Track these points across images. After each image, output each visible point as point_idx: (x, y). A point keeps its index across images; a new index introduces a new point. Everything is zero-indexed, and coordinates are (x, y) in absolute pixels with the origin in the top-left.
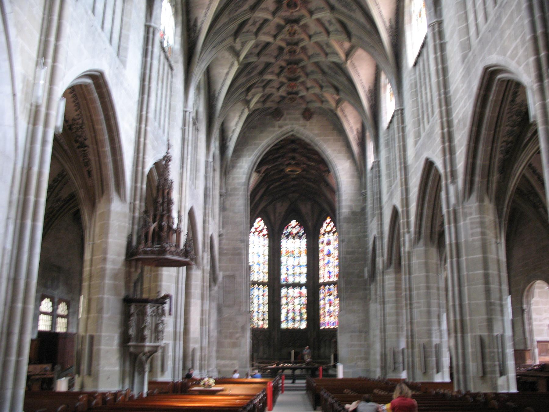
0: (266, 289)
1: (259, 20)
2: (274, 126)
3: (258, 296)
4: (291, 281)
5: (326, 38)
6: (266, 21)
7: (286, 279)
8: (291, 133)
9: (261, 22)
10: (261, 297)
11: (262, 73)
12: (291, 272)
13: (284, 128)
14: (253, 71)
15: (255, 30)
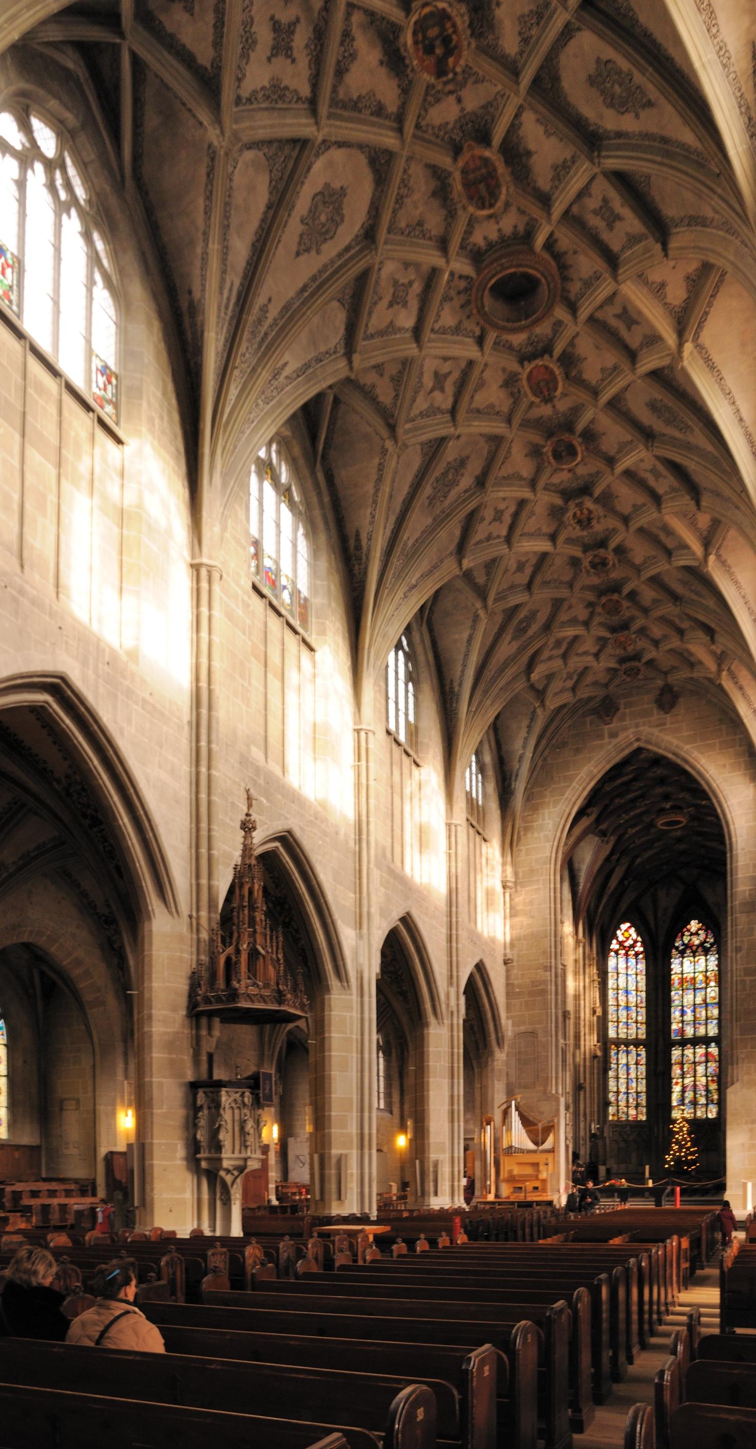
0: (643, 1053)
1: (507, 508)
2: (601, 737)
3: (627, 1065)
4: (689, 1032)
5: (655, 515)
6: (522, 503)
7: (682, 1031)
8: (636, 745)
9: (512, 509)
10: (633, 1067)
11: (547, 627)
12: (689, 1017)
13: (622, 736)
14: (529, 626)
15: (504, 532)
